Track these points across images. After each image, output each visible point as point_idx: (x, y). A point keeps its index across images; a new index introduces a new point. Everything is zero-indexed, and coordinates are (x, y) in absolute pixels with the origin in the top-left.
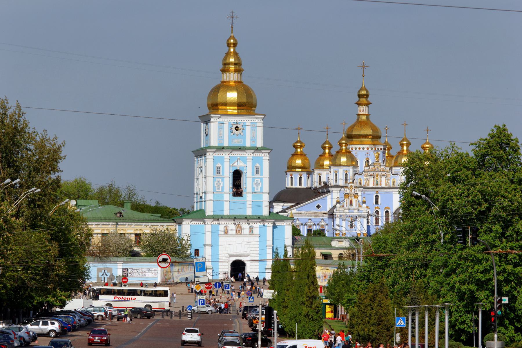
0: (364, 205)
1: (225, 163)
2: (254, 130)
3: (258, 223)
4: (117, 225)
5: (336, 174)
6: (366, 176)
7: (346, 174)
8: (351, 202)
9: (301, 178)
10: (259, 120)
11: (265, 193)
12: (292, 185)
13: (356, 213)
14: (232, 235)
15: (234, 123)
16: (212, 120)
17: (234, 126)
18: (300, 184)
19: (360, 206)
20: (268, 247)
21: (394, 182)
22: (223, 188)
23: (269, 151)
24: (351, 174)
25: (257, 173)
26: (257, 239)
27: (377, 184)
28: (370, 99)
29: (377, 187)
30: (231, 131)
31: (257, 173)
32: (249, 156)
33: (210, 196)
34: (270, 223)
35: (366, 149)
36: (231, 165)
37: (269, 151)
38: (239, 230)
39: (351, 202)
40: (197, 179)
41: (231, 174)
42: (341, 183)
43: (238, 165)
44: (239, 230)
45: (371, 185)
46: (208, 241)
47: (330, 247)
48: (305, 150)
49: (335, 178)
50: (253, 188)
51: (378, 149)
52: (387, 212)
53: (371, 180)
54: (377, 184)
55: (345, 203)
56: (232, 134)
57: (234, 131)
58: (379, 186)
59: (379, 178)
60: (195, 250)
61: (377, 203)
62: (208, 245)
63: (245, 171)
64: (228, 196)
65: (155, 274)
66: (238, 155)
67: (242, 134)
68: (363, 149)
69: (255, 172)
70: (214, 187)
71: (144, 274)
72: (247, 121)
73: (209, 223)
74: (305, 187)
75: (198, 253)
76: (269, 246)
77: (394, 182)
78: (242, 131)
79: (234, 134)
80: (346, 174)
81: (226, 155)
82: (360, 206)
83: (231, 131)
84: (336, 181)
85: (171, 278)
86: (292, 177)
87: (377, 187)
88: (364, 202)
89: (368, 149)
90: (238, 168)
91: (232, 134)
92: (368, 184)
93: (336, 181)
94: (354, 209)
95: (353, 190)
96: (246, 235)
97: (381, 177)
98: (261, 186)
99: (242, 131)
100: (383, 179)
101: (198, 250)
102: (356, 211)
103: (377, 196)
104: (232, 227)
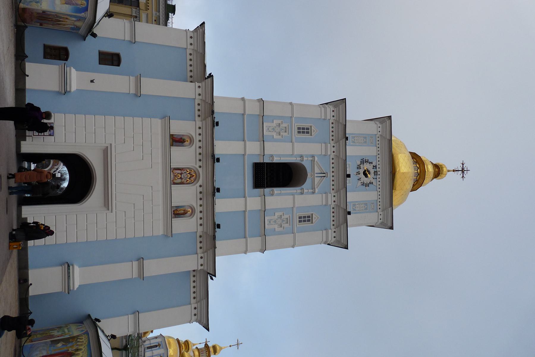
3: (200, 229)
5: (156, 346)
14: (167, 157)
15: (376, 166)
20: (135, 264)
34: (201, 261)
36: (316, 159)
38: (179, 176)
44: (179, 176)
46: (151, 86)
49: (152, 345)
50: (274, 211)
56: (359, 163)
63: (305, 191)
67: (359, 183)
69: (302, 214)
73: (199, 91)
76: (141, 269)
78: (363, 184)
83: (363, 161)
84: (148, 348)
93: (148, 348)
96: (168, 196)
98: (278, 229)
99: (363, 184)
101: (118, 65)
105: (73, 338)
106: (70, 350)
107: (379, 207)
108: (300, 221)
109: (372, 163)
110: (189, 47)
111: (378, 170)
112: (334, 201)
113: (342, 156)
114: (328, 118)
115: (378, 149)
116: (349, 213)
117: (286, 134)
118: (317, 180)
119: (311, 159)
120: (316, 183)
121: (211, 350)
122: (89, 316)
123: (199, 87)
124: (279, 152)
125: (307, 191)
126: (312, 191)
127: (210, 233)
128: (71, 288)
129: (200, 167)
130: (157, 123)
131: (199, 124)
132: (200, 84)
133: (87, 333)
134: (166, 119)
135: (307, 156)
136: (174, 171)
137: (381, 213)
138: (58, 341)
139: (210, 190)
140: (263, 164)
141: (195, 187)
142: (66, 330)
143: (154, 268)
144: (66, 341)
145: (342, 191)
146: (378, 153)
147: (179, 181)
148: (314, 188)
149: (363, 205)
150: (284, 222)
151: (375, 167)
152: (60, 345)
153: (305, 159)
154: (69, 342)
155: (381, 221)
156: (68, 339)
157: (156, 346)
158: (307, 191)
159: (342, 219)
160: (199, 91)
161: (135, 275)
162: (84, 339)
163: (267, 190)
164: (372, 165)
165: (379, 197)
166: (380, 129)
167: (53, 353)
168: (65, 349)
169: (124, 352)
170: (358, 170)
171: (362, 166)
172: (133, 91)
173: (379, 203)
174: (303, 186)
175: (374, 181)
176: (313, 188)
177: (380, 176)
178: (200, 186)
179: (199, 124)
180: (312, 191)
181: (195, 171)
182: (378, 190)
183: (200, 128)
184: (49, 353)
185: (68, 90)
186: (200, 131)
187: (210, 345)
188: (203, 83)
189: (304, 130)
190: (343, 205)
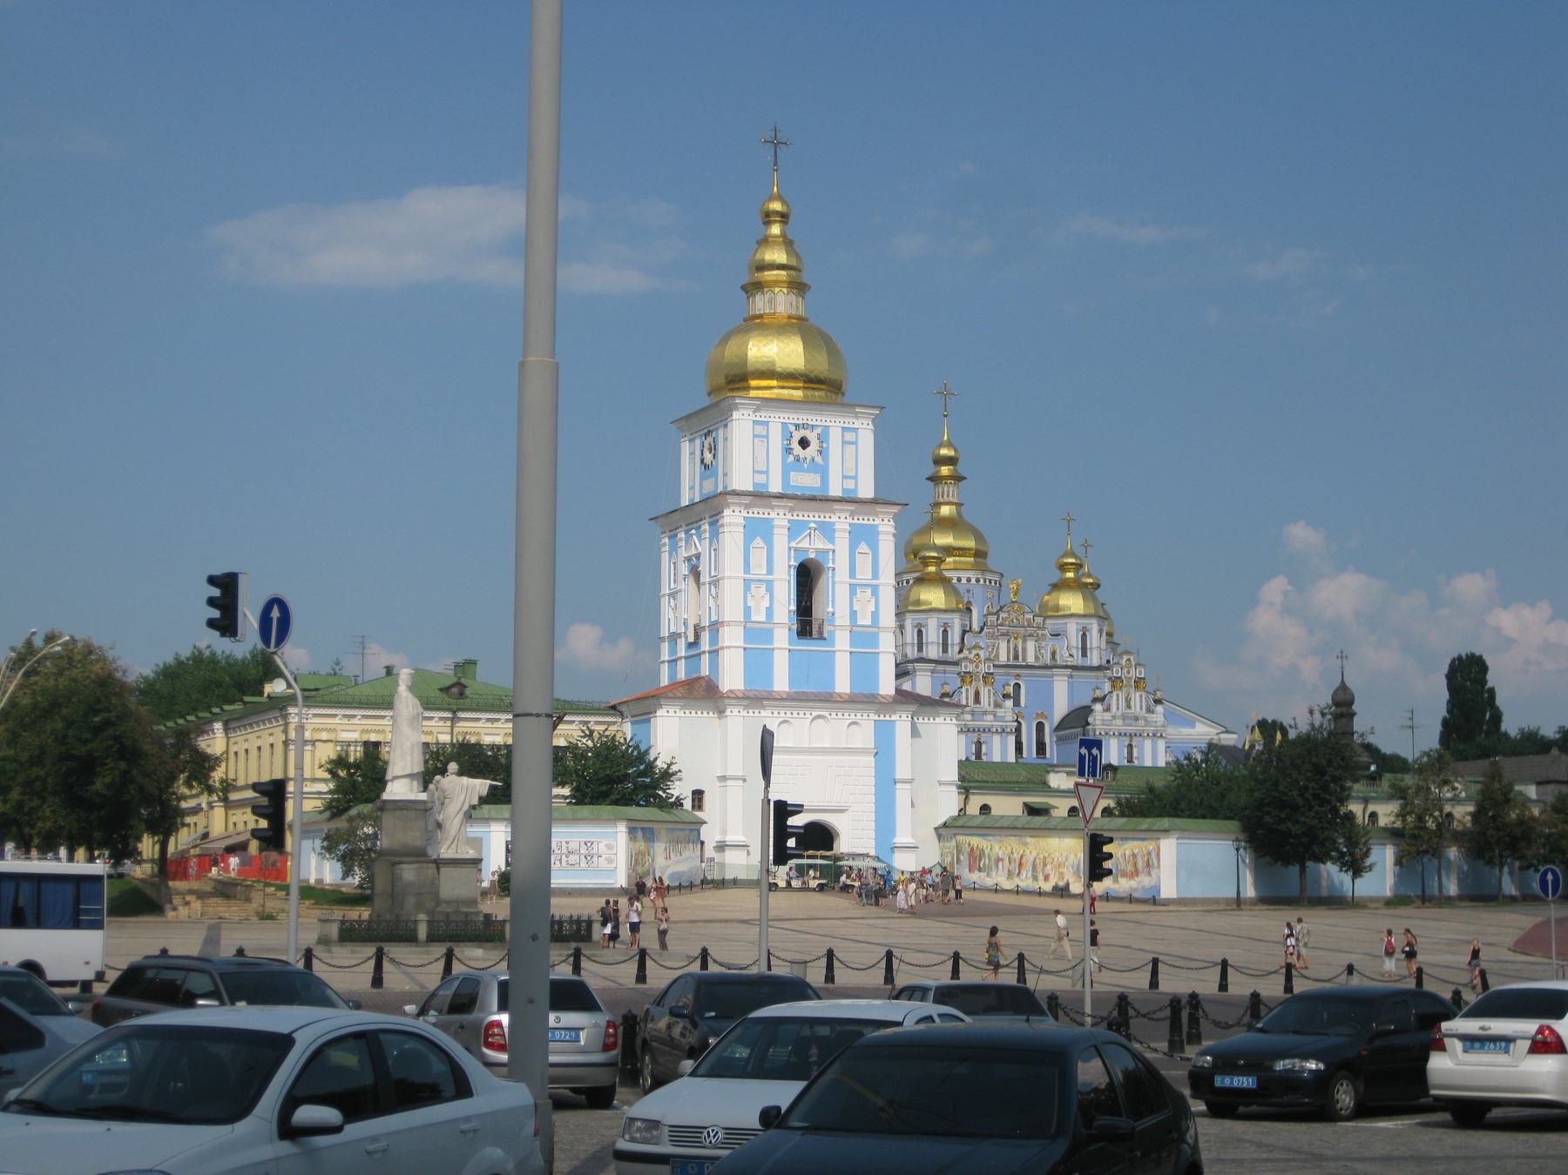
0: (1009, 703)
1: (776, 538)
2: (850, 450)
4: (454, 720)
5: (920, 632)
6: (992, 636)
7: (945, 632)
8: (977, 694)
11: (886, 629)
13: (988, 720)
15: (797, 426)
16: (736, 415)
17: (797, 436)
19: (997, 705)
21: (1054, 654)
23: (895, 509)
24: (954, 636)
27: (1016, 658)
28: (962, 468)
29: (1016, 665)
30: (789, 450)
32: (841, 521)
33: (732, 637)
36: (793, 544)
39: (977, 694)
40: (673, 595)
41: (793, 572)
42: (933, 652)
43: (812, 545)
45: (1003, 658)
47: (1044, 787)
50: (853, 614)
52: (1040, 727)
53: (1003, 646)
54: (1016, 658)
57: (797, 449)
58: (1020, 662)
59: (1020, 641)
61: (1017, 703)
64: (783, 636)
65: (610, 861)
66: (812, 517)
67: (819, 459)
70: (747, 610)
71: (573, 859)
72: (833, 423)
75: (701, 800)
77: (1054, 654)
78: (820, 452)
79: (797, 459)
80: (945, 632)
81: (780, 518)
82: (997, 705)
83: (788, 450)
84: (920, 649)
85: (647, 873)
87: (1016, 665)
88: (1006, 696)
89: (969, 580)
90: (812, 556)
91: (791, 458)
92: (997, 656)
93: (920, 649)
94: (985, 713)
95: (981, 666)
97: (1024, 641)
100: (1031, 645)
102: (990, 717)
103: (1017, 686)
114: (742, 521)
120: (821, 546)
121: (945, 470)
144: (959, 852)
157: (920, 632)
161: (908, 786)
162: (960, 838)
166: (746, 412)
175: (819, 430)
176: (827, 551)
187: (930, 469)
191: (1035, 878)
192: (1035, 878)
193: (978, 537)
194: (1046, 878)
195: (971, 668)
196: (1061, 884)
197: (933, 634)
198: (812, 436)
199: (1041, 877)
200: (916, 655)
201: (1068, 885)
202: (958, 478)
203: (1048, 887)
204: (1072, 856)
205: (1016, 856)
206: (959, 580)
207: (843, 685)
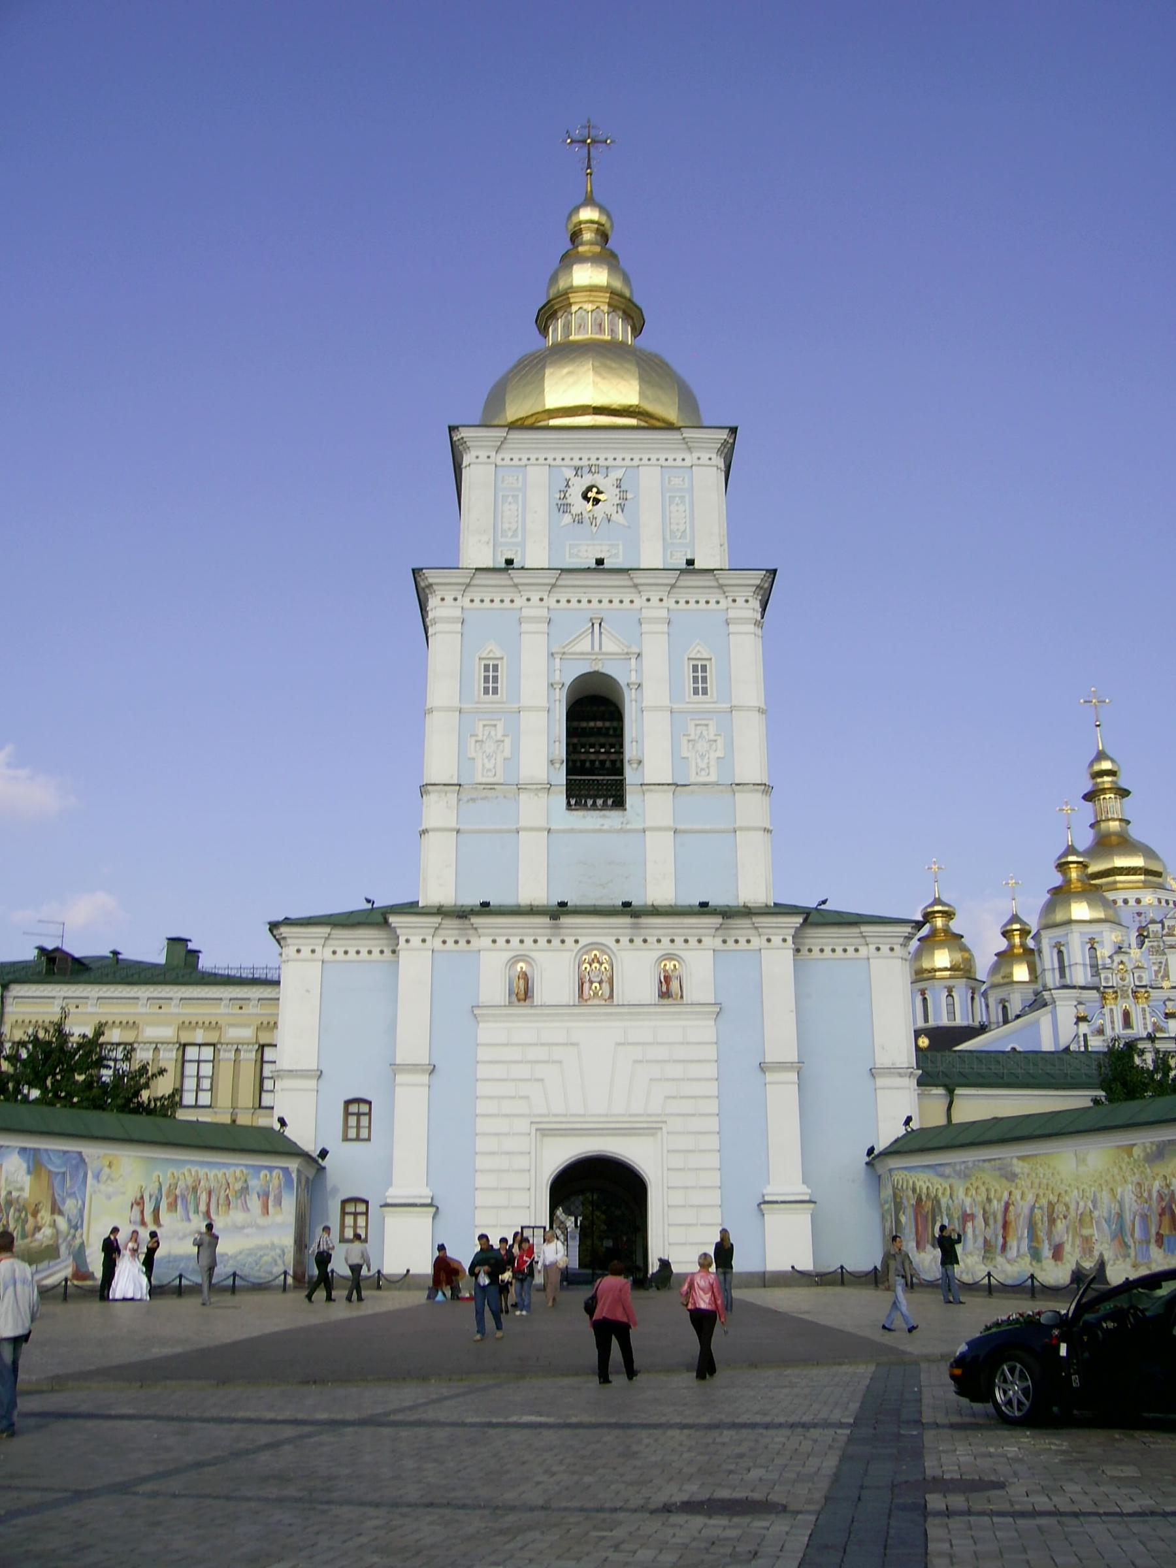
5: (1060, 952)
8: (1126, 1015)
9: (950, 995)
10: (705, 456)
12: (926, 1020)
15: (577, 470)
18: (952, 1014)
20: (770, 1077)
22: (512, 761)
25: (700, 685)
26: (704, 1029)
31: (700, 685)
32: (654, 608)
34: (776, 940)
35: (1132, 902)
37: (756, 578)
39: (1126, 1015)
46: (412, 1043)
48: (955, 926)
49: (1056, 965)
51: (1167, 902)
55: (1108, 1017)
56: (567, 519)
57: (579, 506)
60: (348, 1103)
62: (414, 1068)
63: (633, 678)
67: (618, 518)
68: (1126, 902)
73: (416, 941)
74: (965, 1023)
76: (782, 1066)
78: (621, 507)
79: (579, 519)
81: (532, 605)
84: (1062, 975)
86: (925, 1000)
90: (596, 669)
93: (1062, 975)
101: (370, 1103)
104: (555, 967)
105: (895, 1195)
106: (913, 1202)
107: (679, 463)
108: (705, 692)
109: (568, 481)
110: (318, 955)
111: (584, 462)
112: (661, 600)
113: (550, 578)
115: (533, 461)
116: (690, 562)
117: (500, 726)
118: (609, 646)
119: (558, 660)
122: (867, 1164)
123: (407, 941)
124: (542, 744)
125: (633, 673)
126: (633, 661)
127: (718, 920)
128: (807, 1198)
129: (577, 941)
130: (488, 1031)
131: (486, 941)
132: (402, 940)
133: (890, 1170)
134: (476, 1012)
135: (550, 670)
136: (586, 996)
137: (695, 455)
138: (898, 1221)
139: (627, 920)
140: (569, 783)
141: (617, 953)
142: (886, 1207)
143: (781, 1042)
144: (898, 1206)
145: (637, 581)
146: (541, 461)
147: (606, 986)
148: (627, 654)
149: (674, 508)
150: (705, 733)
151: (577, 470)
152: (903, 1219)
153: (557, 677)
154: (901, 1203)
155: (714, 456)
156: (896, 1204)
157: (1060, 952)
158: (633, 673)
159: (706, 580)
160: (416, 941)
163: (630, 775)
164: (575, 481)
165: (653, 461)
166: (483, 454)
167: (914, 1230)
168: (910, 1211)
169: (956, 1092)
170: (586, 521)
171: (575, 510)
172: (425, 1078)
173: (670, 463)
174: (622, 681)
177: (602, 458)
178: (618, 941)
179: (486, 941)
180: (633, 661)
181: (586, 953)
182: (636, 462)
183: (494, 941)
184: (913, 1236)
185: (429, 1201)
186: (501, 941)
187: (1088, 786)
188: (399, 931)
189: (491, 679)
190: (670, 578)
191: (1036, 1255)
192: (1036, 1255)
193: (1148, 853)
194: (1057, 1253)
195: (1114, 981)
196: (1088, 1265)
197: (1077, 953)
198: (606, 483)
199: (1047, 1252)
200: (1058, 985)
201: (1102, 1266)
202: (1123, 793)
203: (1056, 1274)
204: (1105, 1196)
205: (997, 1206)
206: (1126, 902)
207: (660, 893)
